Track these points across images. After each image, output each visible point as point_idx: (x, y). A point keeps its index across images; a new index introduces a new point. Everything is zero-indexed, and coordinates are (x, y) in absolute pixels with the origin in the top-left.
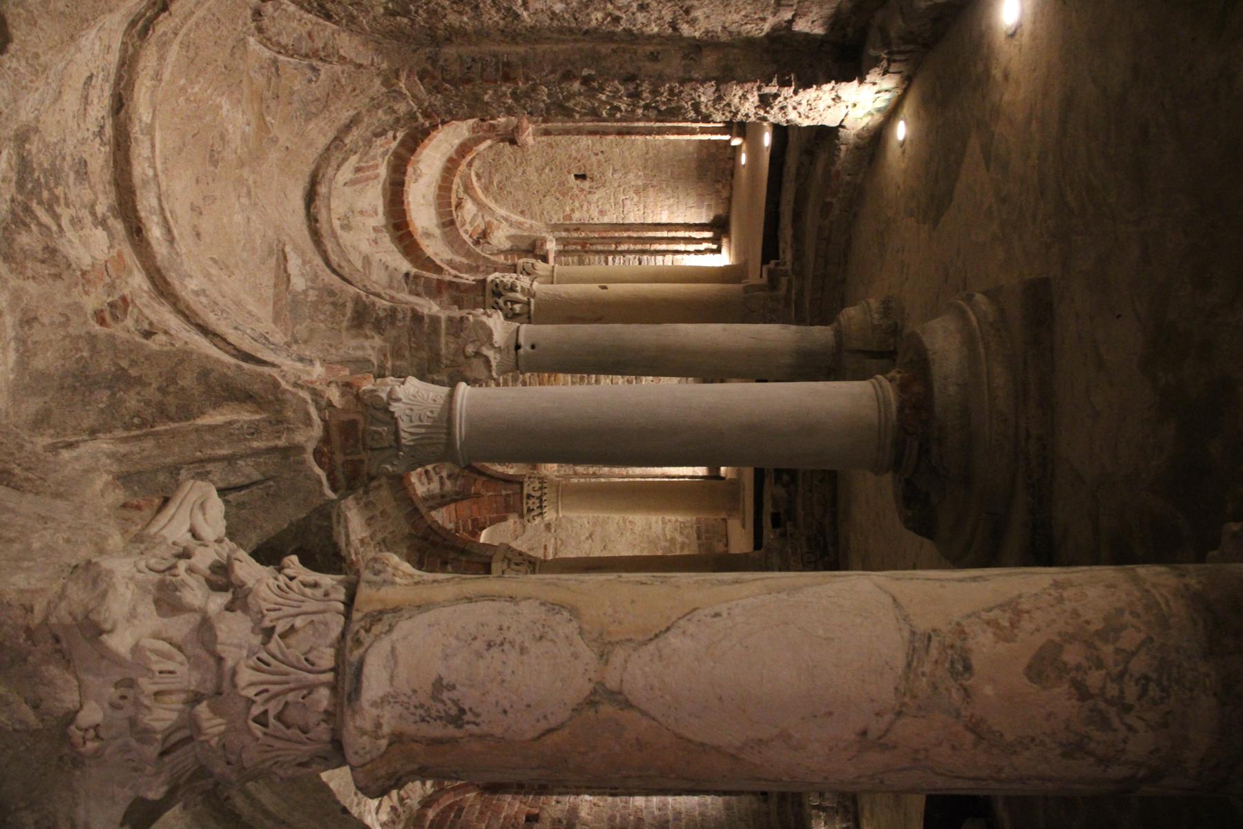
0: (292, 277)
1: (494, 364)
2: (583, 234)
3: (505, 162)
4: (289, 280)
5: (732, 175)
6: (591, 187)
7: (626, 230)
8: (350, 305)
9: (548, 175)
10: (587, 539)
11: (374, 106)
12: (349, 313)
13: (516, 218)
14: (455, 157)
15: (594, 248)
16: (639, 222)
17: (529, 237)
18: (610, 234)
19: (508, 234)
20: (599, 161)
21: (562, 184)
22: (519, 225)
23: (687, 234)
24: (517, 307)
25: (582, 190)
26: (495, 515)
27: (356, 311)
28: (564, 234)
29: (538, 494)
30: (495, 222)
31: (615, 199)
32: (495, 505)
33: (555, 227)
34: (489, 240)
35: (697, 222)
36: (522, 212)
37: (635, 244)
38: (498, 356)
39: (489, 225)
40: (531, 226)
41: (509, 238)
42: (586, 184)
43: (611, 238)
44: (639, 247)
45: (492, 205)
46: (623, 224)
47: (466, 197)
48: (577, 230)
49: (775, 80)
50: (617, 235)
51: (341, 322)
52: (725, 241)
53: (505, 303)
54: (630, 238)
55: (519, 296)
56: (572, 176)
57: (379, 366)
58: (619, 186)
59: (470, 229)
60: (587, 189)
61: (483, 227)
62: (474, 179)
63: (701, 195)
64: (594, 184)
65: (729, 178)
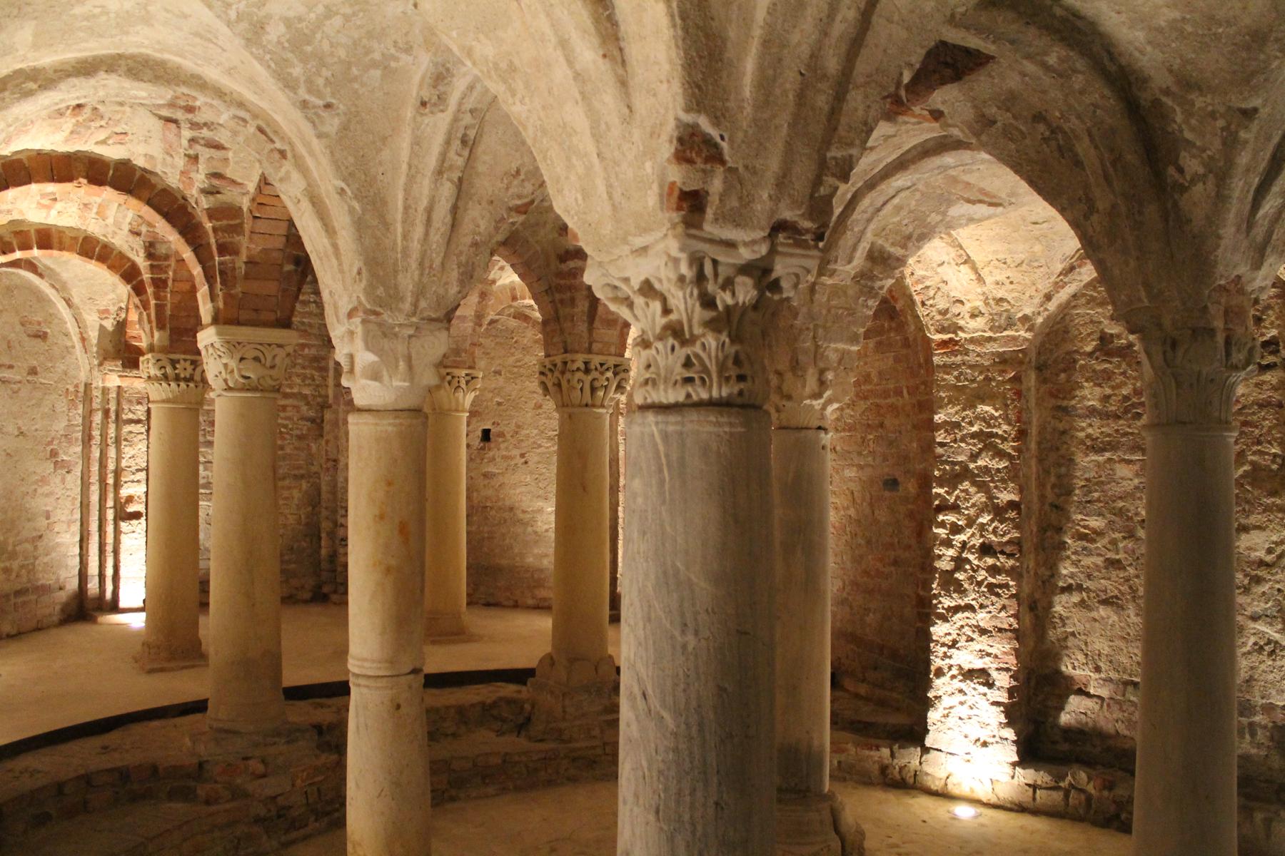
0: (970, 205)
1: (814, 403)
3: (513, 354)
4: (969, 201)
5: (488, 605)
8: (898, 251)
9: (491, 399)
10: (19, 428)
11: (987, 298)
12: (892, 250)
24: (601, 393)
26: (168, 313)
27: (890, 256)
29: (197, 377)
32: (183, 314)
38: (817, 407)
49: (1014, 683)
51: (887, 240)
53: (608, 379)
55: (611, 395)
57: (835, 271)
65: (482, 601)
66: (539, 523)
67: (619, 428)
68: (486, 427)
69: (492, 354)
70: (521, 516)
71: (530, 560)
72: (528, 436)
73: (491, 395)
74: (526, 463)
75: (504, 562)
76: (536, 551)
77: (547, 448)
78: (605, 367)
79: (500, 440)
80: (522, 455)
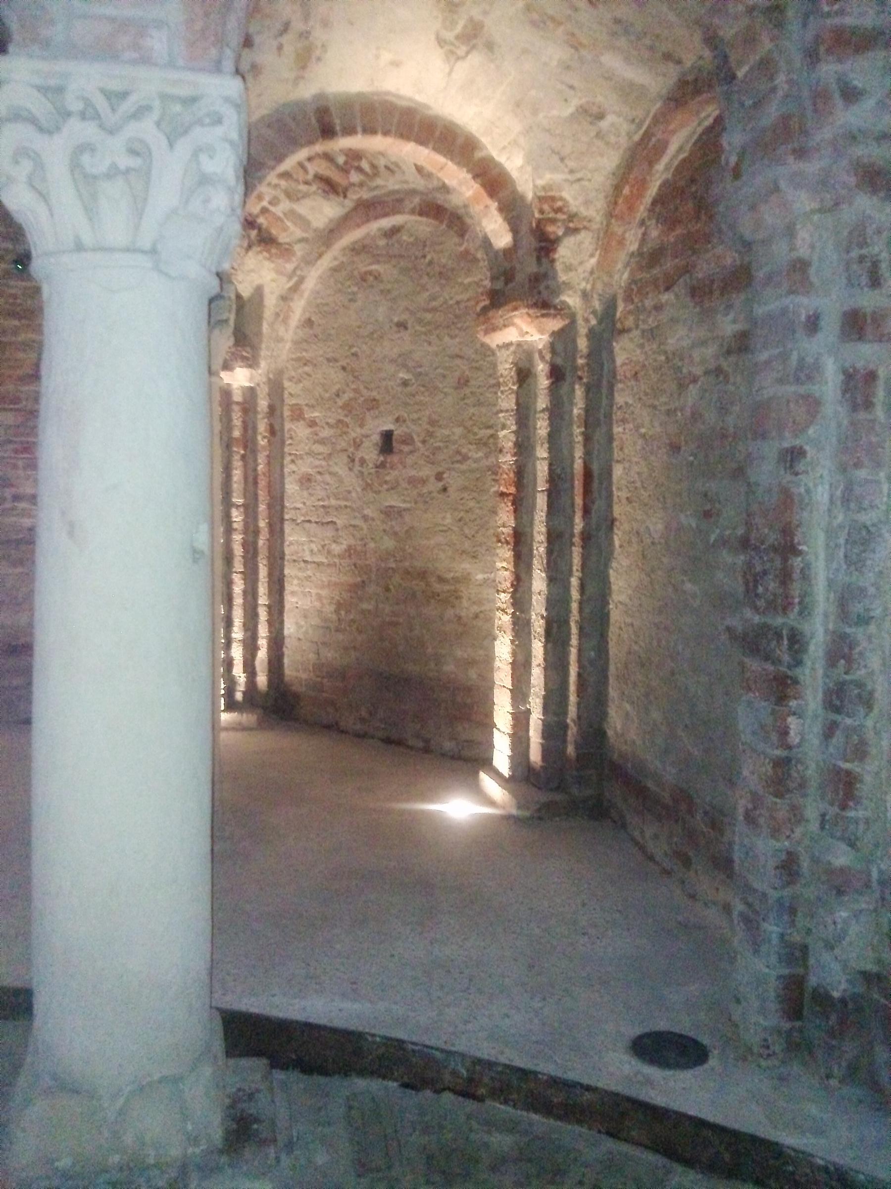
2: (262, 442)
3: (424, 288)
5: (388, 741)
6: (363, 462)
7: (270, 525)
13: (299, 308)
14: (478, 155)
15: (237, 463)
16: (287, 551)
17: (259, 334)
18: (262, 495)
19: (267, 290)
20: (424, 481)
21: (373, 404)
22: (282, 316)
23: (263, 643)
25: (357, 445)
28: (263, 404)
30: (290, 267)
31: (338, 508)
33: (276, 388)
34: (256, 249)
35: (286, 661)
36: (309, 323)
37: (245, 545)
39: (286, 251)
40: (280, 340)
41: (259, 291)
42: (370, 453)
43: (256, 495)
44: (238, 551)
45: (326, 262)
46: (282, 520)
47: (349, 204)
48: (272, 431)
50: (262, 507)
52: (248, 718)
54: (256, 532)
56: (389, 426)
58: (365, 518)
59: (278, 210)
60: (359, 455)
61: (283, 238)
62: (386, 223)
63: (340, 674)
64: (370, 468)
66: (465, 603)
67: (576, 411)
68: (387, 427)
69: (395, 293)
70: (437, 587)
71: (449, 667)
72: (447, 440)
73: (391, 368)
74: (445, 489)
75: (412, 668)
76: (459, 653)
77: (476, 461)
78: (127, 106)
79: (406, 449)
80: (439, 477)
